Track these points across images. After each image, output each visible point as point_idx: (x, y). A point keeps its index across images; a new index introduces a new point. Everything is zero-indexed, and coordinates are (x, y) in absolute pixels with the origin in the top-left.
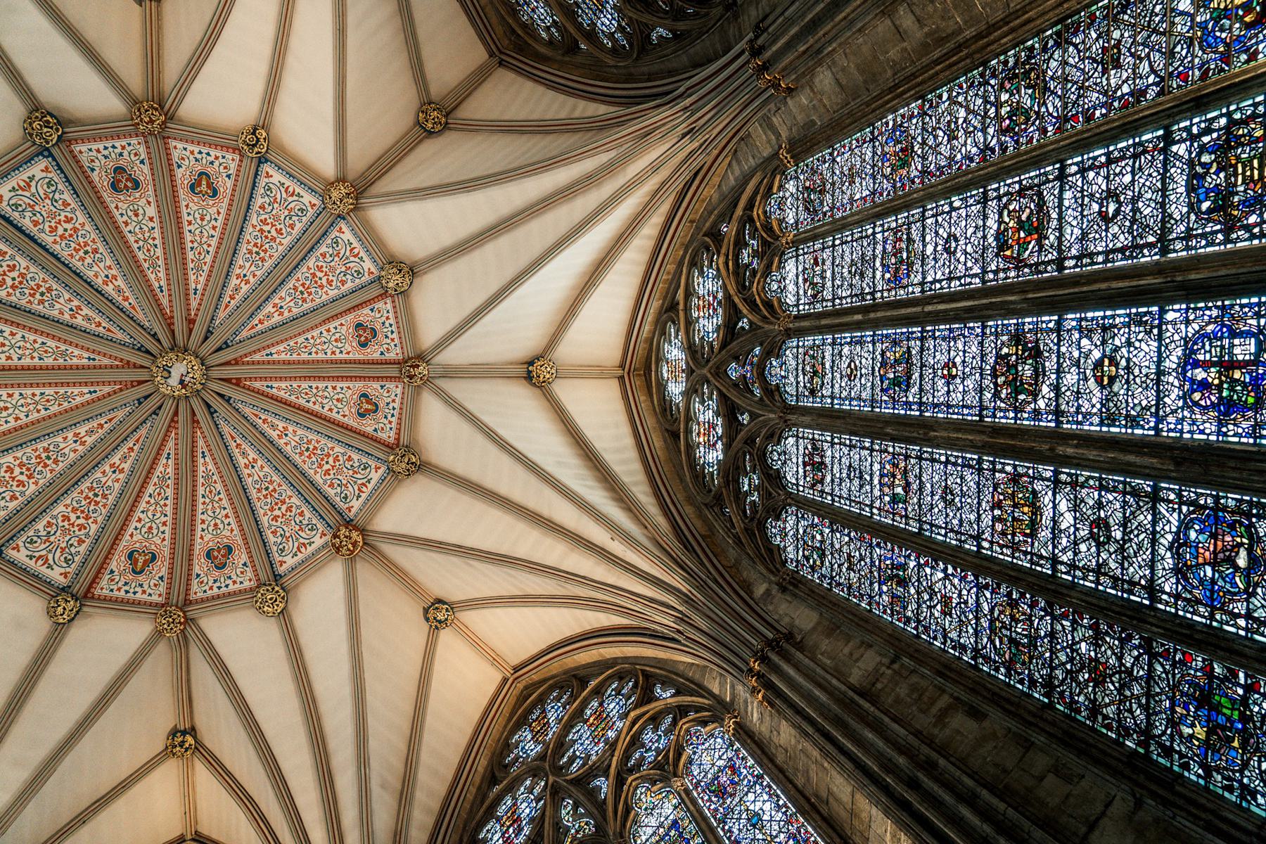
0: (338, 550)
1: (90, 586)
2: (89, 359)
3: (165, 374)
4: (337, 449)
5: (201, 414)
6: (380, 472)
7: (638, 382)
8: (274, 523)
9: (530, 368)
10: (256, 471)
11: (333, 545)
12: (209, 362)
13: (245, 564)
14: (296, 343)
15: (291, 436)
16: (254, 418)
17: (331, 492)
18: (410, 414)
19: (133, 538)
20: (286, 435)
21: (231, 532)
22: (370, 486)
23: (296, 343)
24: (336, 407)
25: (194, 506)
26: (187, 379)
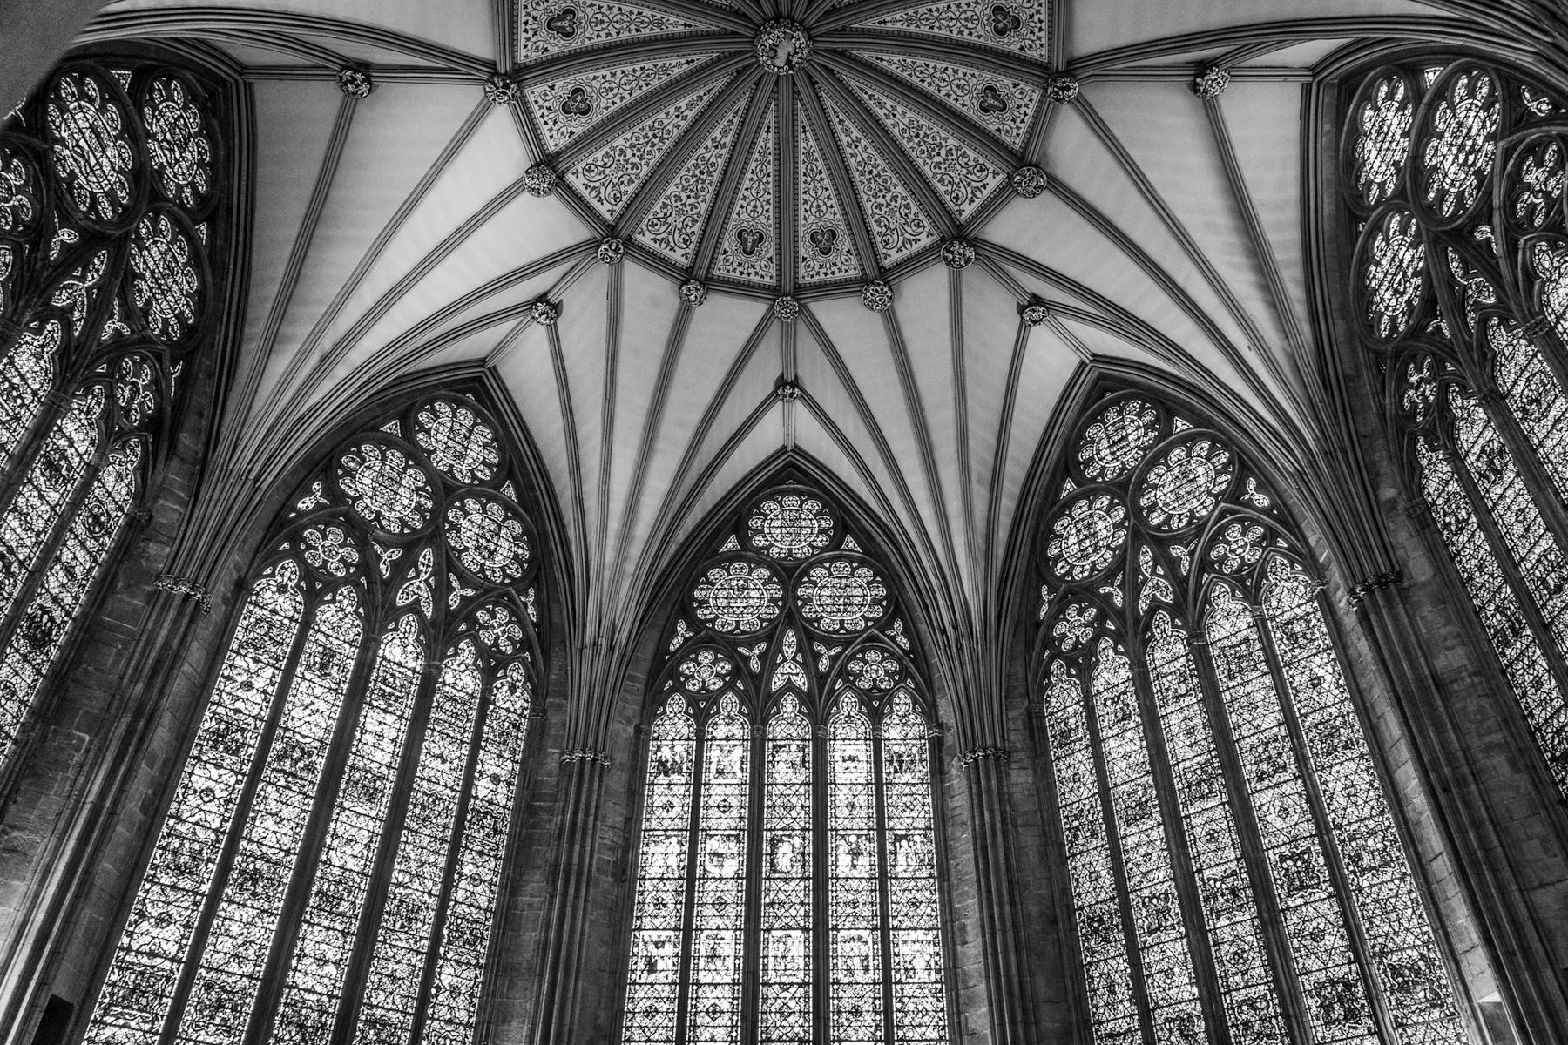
0: (949, 263)
1: (709, 267)
2: (685, 25)
3: (772, 54)
4: (951, 141)
5: (802, 86)
6: (999, 178)
7: (1328, 99)
8: (878, 211)
9: (1198, 80)
10: (860, 151)
11: (945, 258)
12: (809, 21)
13: (849, 252)
14: (916, 13)
15: (899, 117)
16: (859, 92)
17: (941, 189)
18: (1040, 126)
19: (740, 218)
20: (894, 116)
21: (833, 217)
22: (986, 193)
23: (916, 13)
24: (955, 93)
25: (796, 185)
26: (795, 60)
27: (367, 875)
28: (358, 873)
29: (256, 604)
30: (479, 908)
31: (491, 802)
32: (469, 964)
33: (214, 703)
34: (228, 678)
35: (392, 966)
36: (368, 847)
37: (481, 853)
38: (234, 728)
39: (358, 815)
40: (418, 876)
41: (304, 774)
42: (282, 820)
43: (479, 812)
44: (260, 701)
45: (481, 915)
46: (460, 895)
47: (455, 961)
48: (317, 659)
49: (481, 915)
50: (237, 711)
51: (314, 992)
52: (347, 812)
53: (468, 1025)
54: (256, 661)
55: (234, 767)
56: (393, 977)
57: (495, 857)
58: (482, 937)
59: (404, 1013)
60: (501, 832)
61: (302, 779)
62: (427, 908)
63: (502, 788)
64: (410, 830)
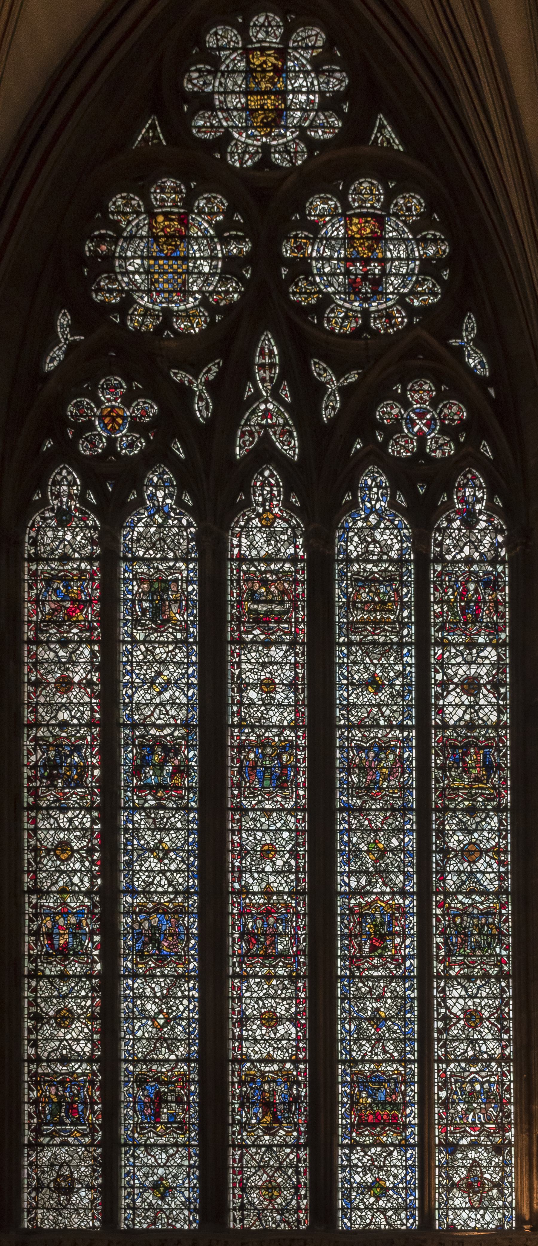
27: (303, 893)
28: (290, 894)
29: (37, 559)
30: (485, 893)
31: (471, 726)
32: (486, 976)
33: (30, 726)
34: (37, 684)
35: (370, 1005)
36: (293, 853)
37: (471, 811)
38: (67, 750)
39: (268, 812)
40: (378, 872)
41: (177, 781)
42: (167, 852)
43: (454, 747)
44: (87, 699)
45: (492, 903)
46: (451, 881)
47: (464, 977)
48: (145, 605)
49: (492, 903)
50: (63, 725)
51: (272, 1061)
52: (251, 815)
53: (503, 1059)
54: (64, 643)
55: (84, 803)
56: (376, 1019)
57: (497, 809)
58: (501, 933)
59: (403, 1061)
60: (499, 767)
61: (177, 788)
62: (404, 914)
63: (486, 697)
64: (349, 809)
